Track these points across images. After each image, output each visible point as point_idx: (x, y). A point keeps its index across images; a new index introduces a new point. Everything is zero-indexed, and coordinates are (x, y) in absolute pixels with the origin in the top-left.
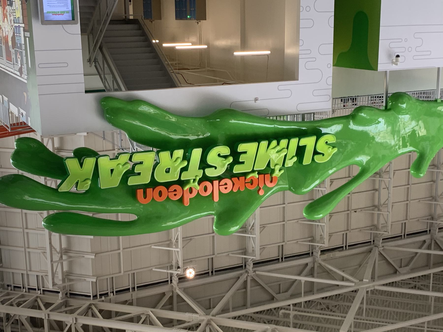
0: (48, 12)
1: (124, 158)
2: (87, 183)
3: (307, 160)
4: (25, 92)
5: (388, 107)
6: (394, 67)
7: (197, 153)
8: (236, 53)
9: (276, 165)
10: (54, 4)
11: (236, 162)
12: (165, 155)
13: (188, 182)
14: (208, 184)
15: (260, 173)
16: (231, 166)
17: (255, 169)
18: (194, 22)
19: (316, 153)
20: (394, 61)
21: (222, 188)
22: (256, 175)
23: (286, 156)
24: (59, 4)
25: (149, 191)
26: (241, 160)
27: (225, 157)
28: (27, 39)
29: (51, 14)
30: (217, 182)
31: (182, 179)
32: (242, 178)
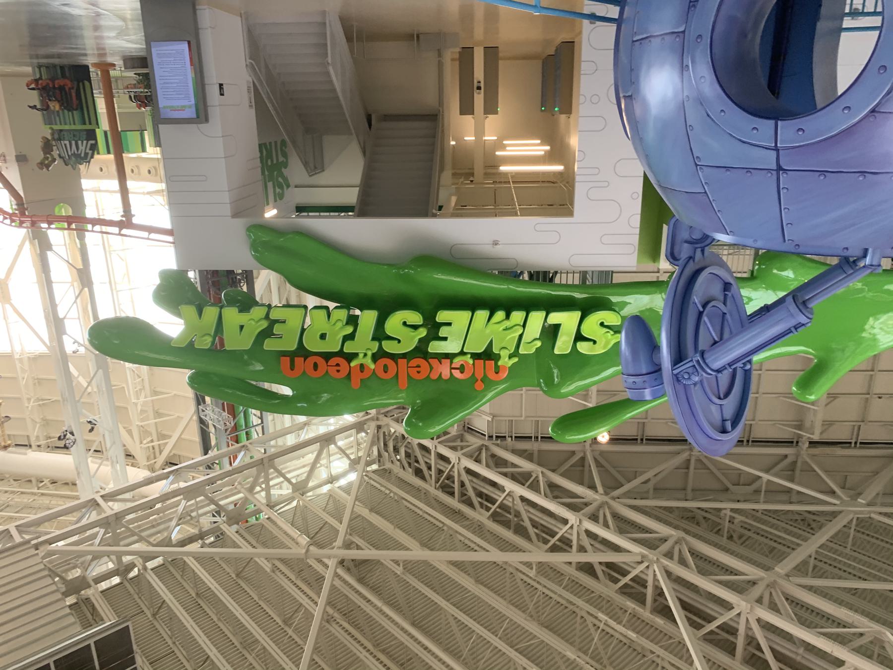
0: (164, 107)
13: (355, 355)
15: (475, 356)
16: (424, 342)
17: (465, 350)
19: (579, 337)
23: (521, 336)
26: (440, 335)
27: (415, 327)
29: (168, 110)
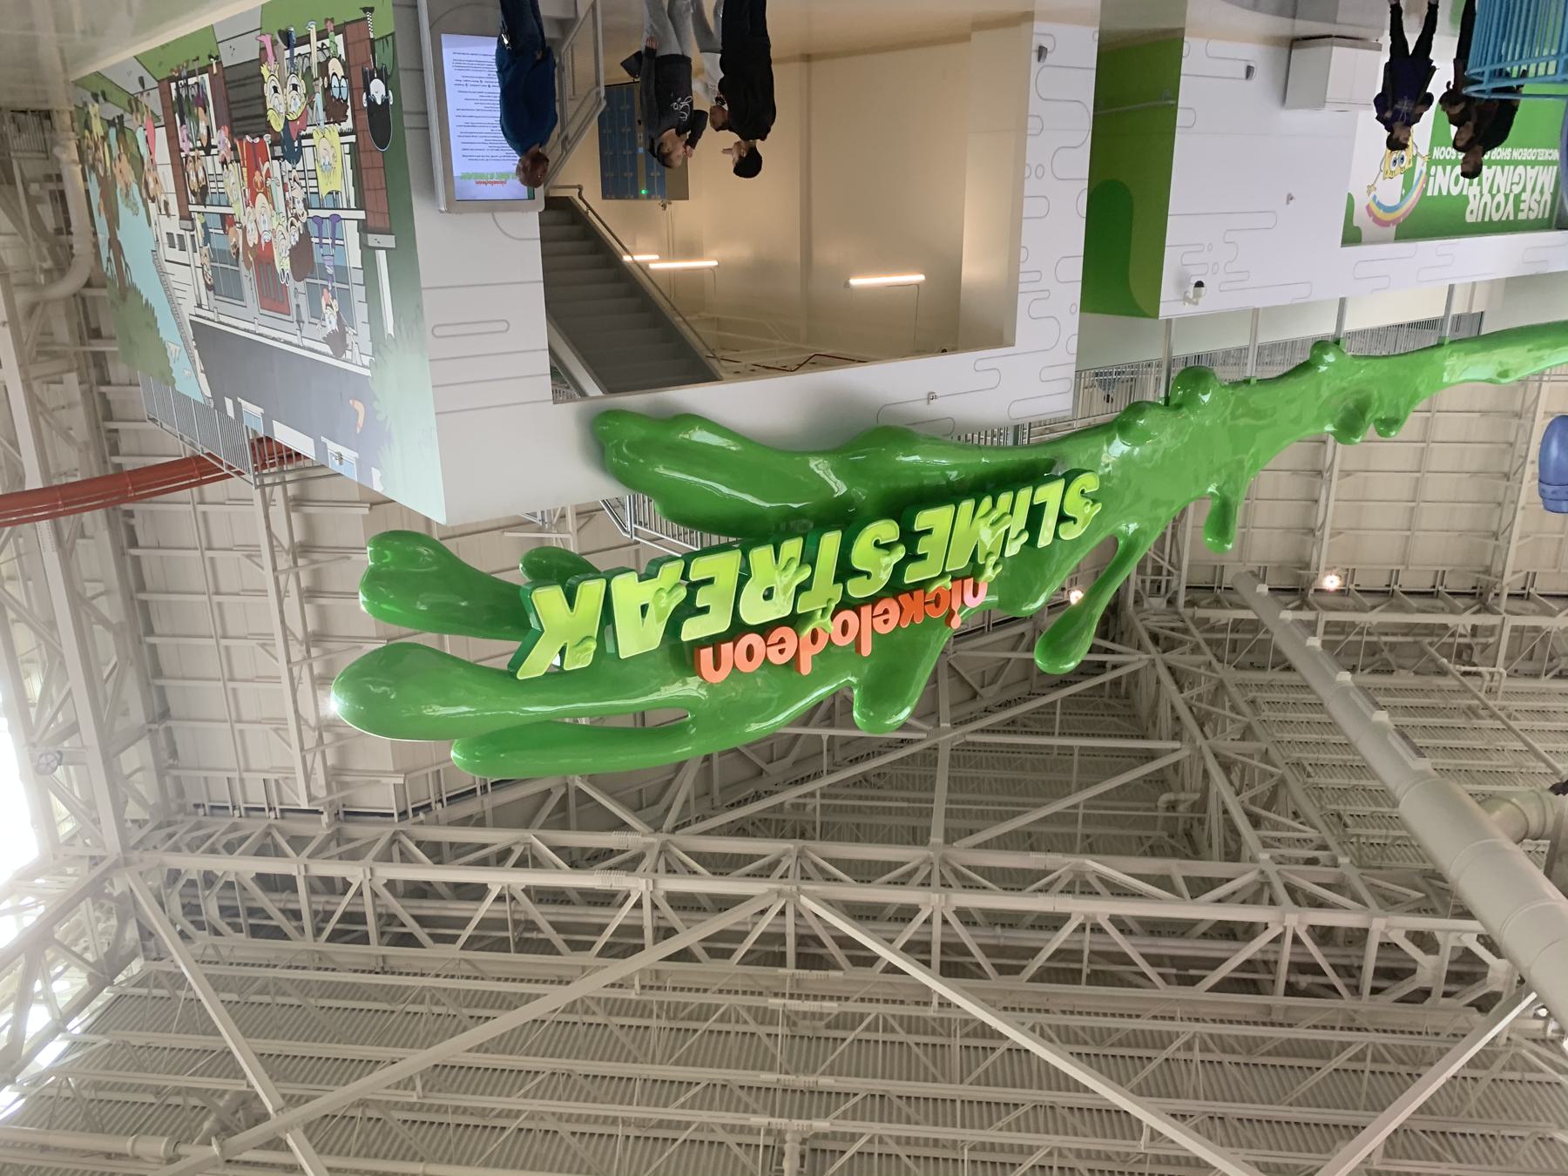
0: (463, 177)
1: (671, 572)
2: (587, 649)
3: (1045, 538)
4: (355, 398)
5: (1173, 402)
6: (1188, 310)
7: (830, 543)
8: (855, 282)
9: (989, 554)
10: (481, 153)
11: (912, 557)
12: (761, 556)
13: (808, 616)
14: (848, 615)
15: (957, 577)
16: (899, 569)
17: (947, 570)
18: (655, 204)
19: (1062, 518)
20: (1191, 295)
21: (878, 621)
22: (947, 583)
23: (1007, 531)
24: (494, 153)
25: (727, 648)
26: (920, 552)
27: (888, 547)
28: (382, 255)
29: (473, 182)
30: (870, 607)
31: (799, 611)
32: (918, 594)
